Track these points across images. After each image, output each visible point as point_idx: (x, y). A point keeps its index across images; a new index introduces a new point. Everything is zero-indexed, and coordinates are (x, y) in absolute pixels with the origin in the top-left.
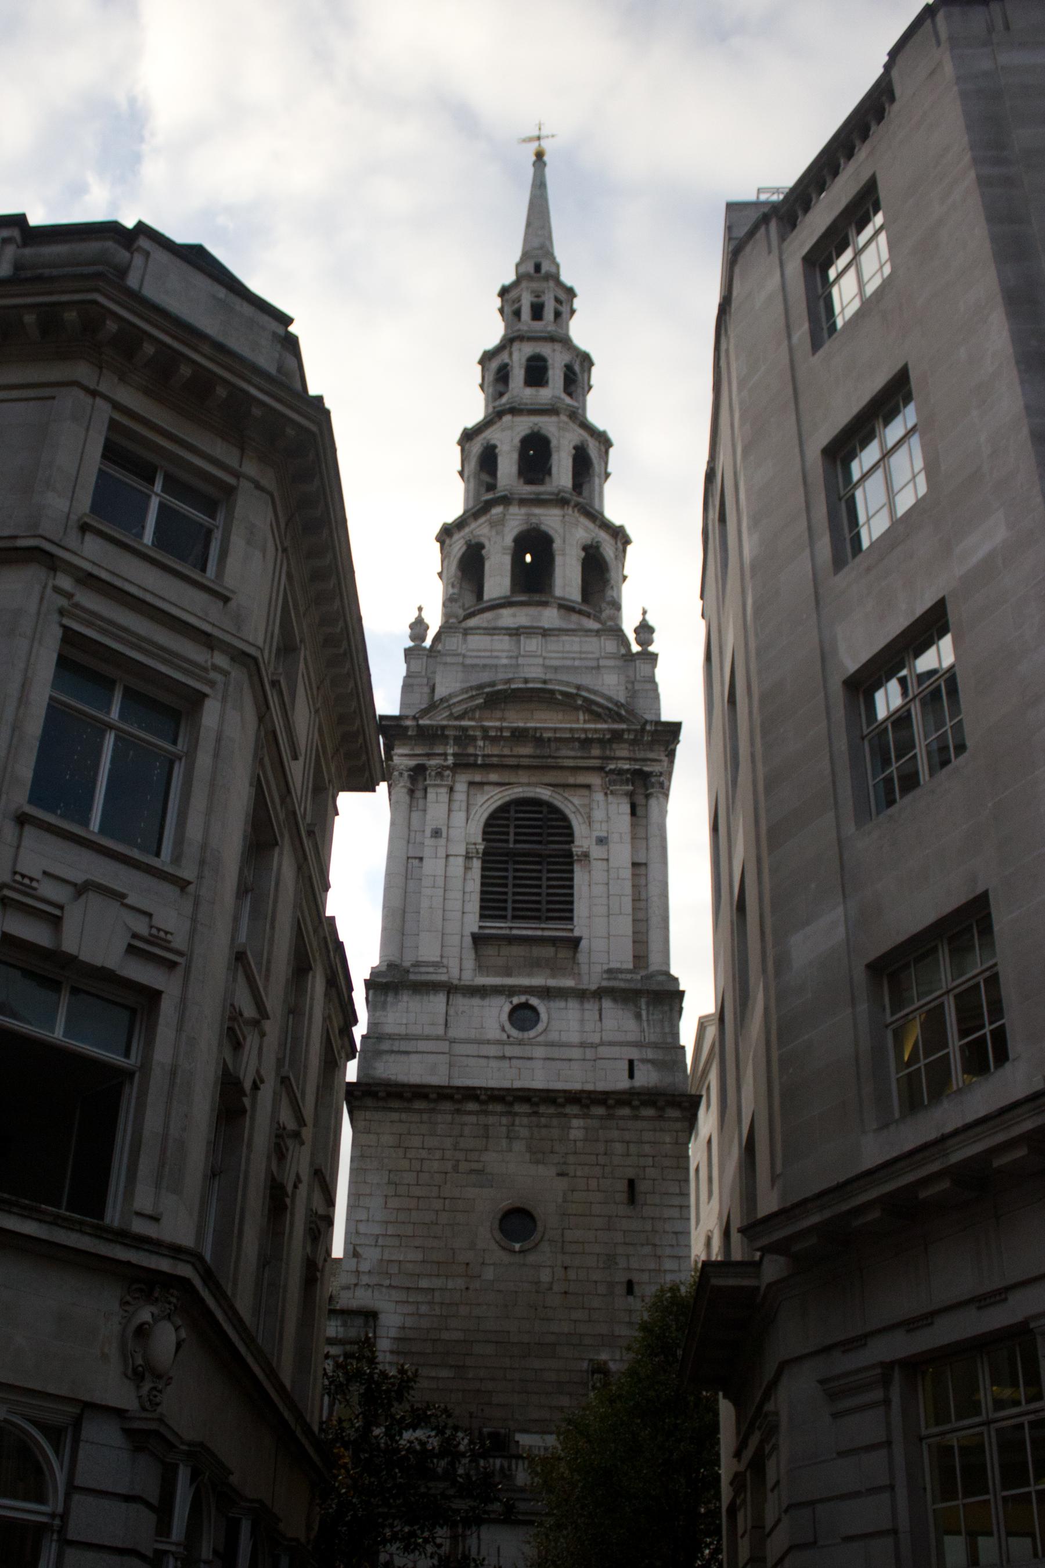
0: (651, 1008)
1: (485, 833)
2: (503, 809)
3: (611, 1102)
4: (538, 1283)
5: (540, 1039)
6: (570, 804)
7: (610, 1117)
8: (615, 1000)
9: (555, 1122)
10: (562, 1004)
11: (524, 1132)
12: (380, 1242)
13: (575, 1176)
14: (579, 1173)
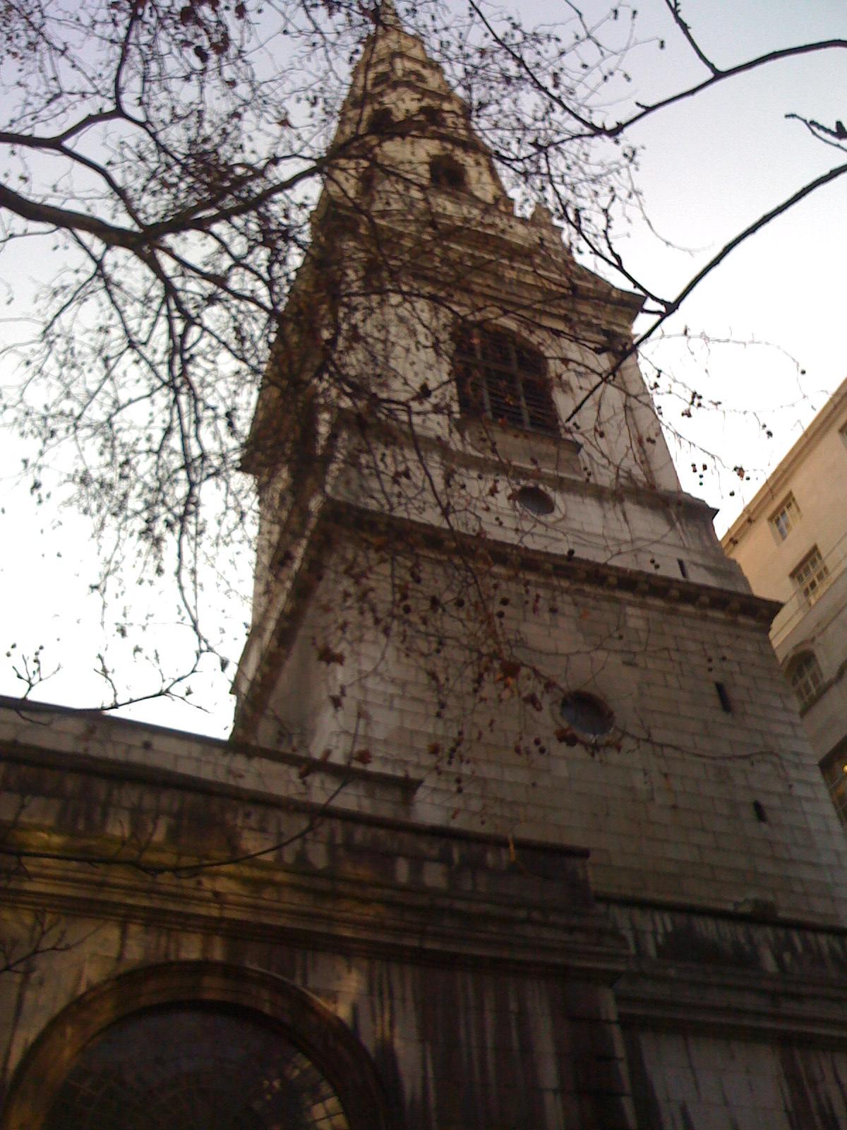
0: (683, 520)
3: (674, 593)
4: (632, 789)
7: (673, 612)
8: (639, 503)
9: (605, 605)
10: (579, 499)
11: (569, 609)
12: (397, 703)
13: (646, 668)
14: (650, 665)
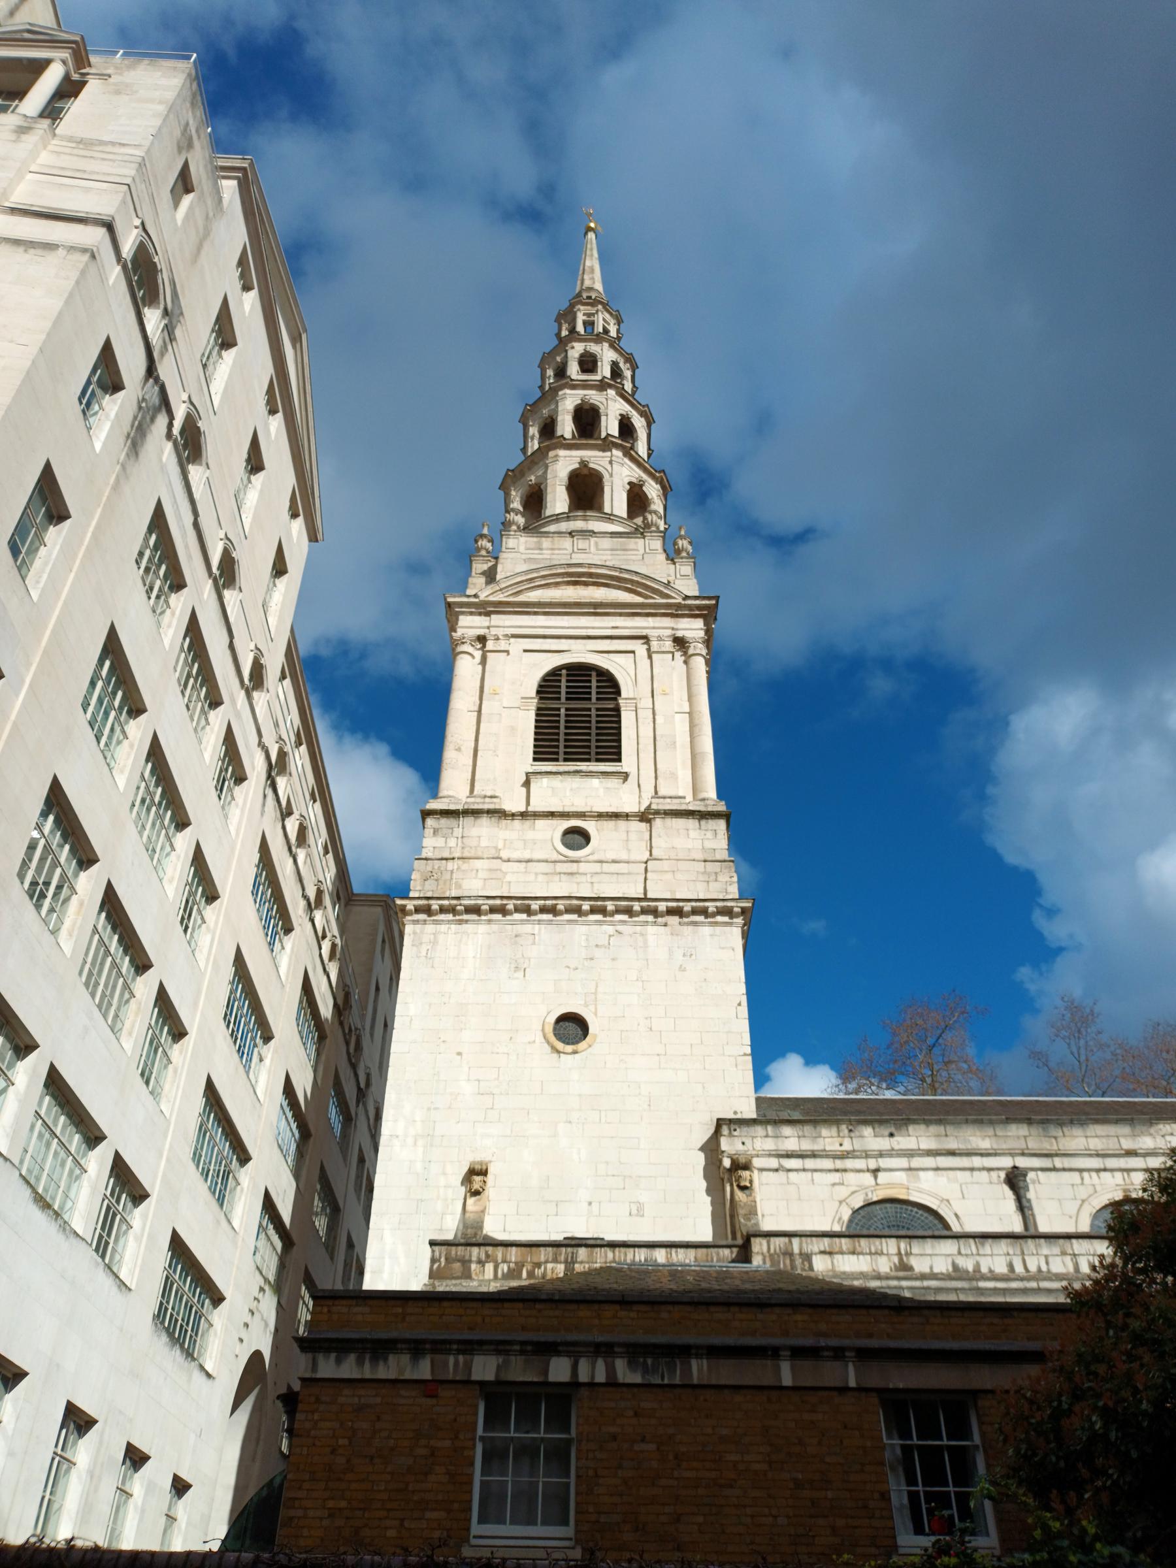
1: (538, 692)
2: (554, 674)
5: (591, 858)
6: (618, 667)
